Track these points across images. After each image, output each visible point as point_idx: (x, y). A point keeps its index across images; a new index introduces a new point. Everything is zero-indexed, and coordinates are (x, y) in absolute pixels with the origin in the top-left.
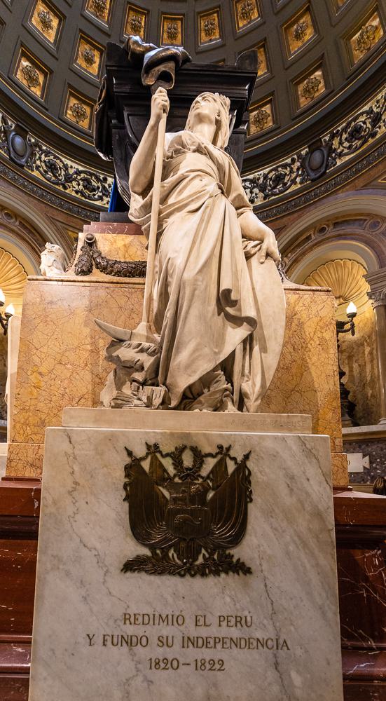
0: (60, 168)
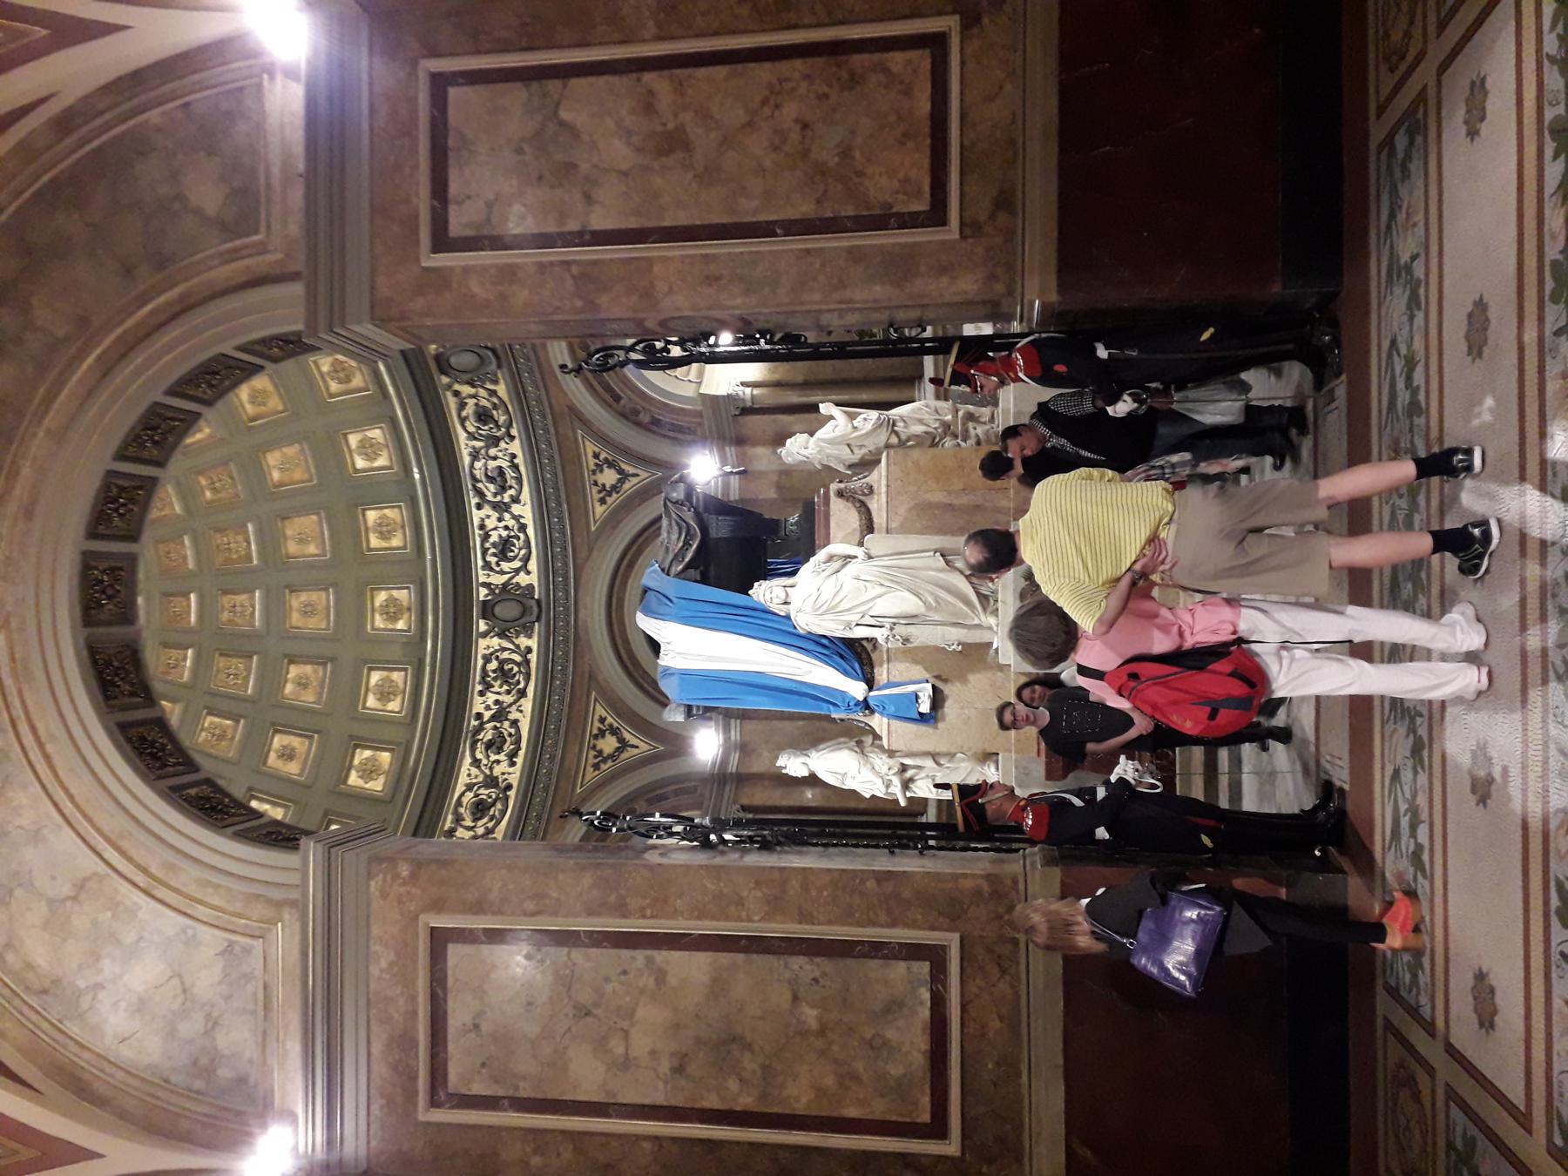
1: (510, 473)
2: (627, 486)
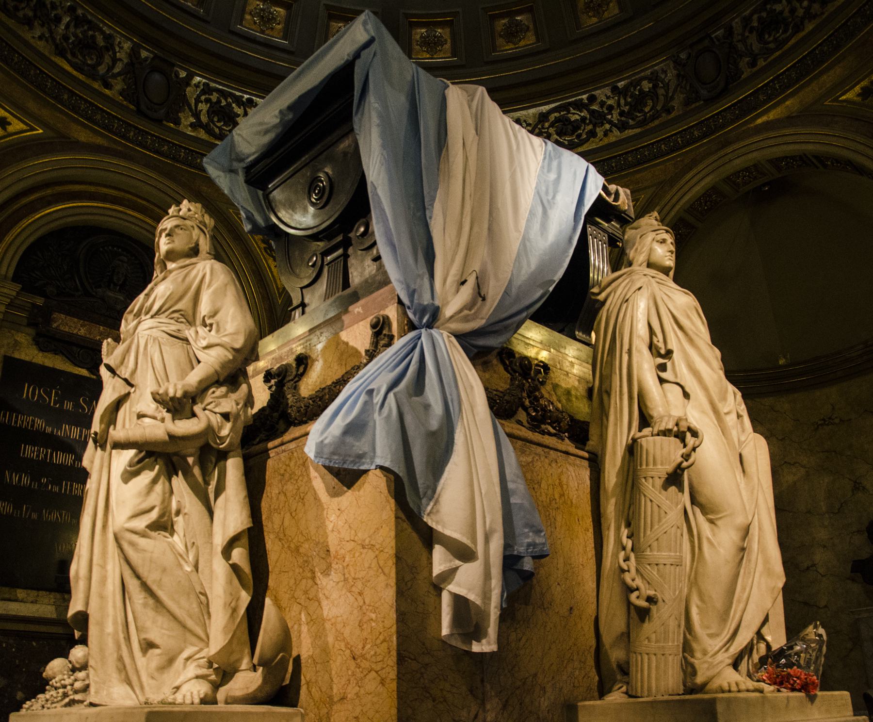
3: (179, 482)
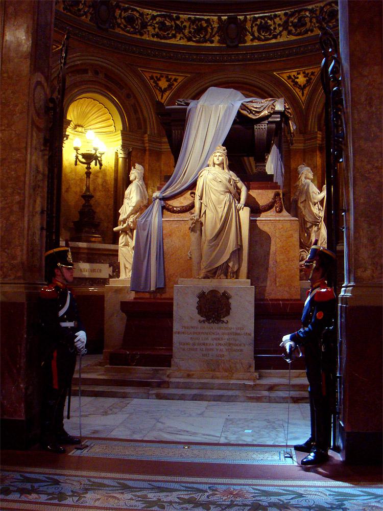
0: (137, 18)
1: (303, 29)
2: (297, 90)
3: (128, 236)
